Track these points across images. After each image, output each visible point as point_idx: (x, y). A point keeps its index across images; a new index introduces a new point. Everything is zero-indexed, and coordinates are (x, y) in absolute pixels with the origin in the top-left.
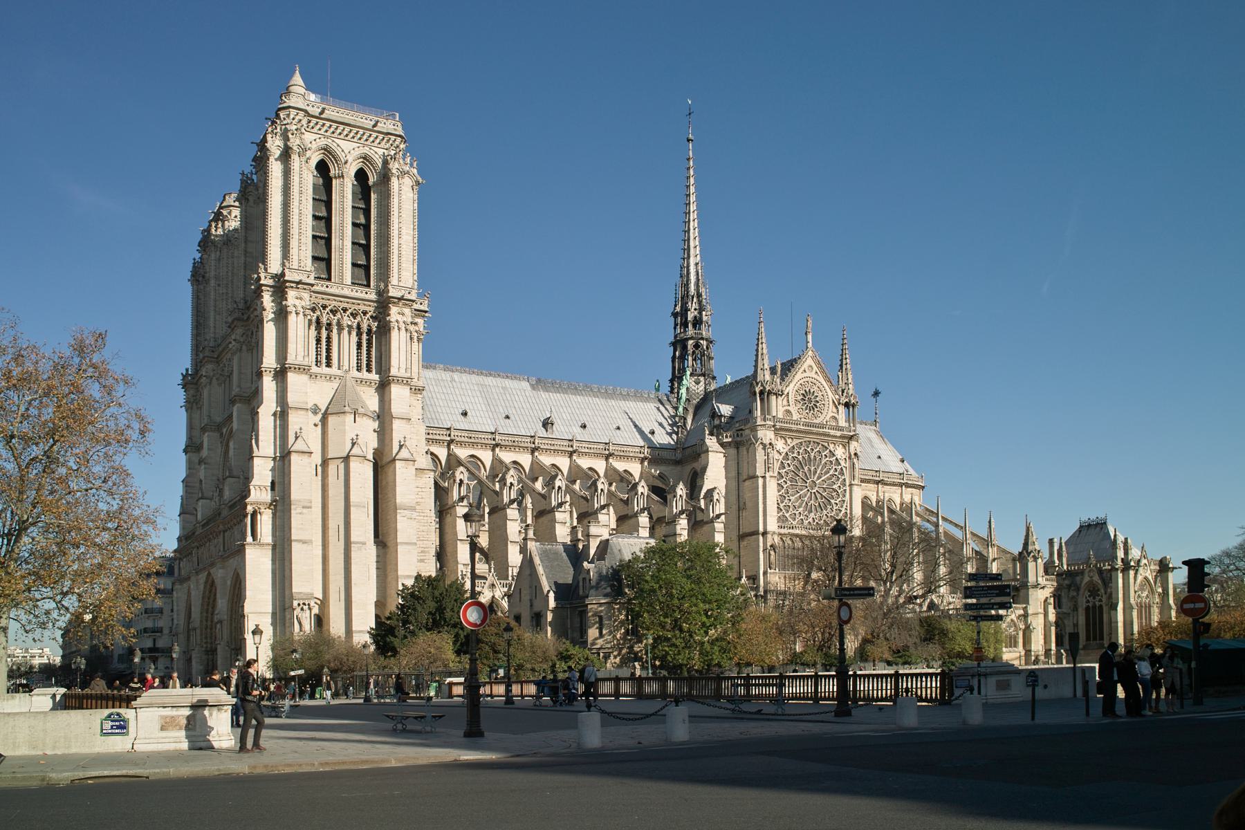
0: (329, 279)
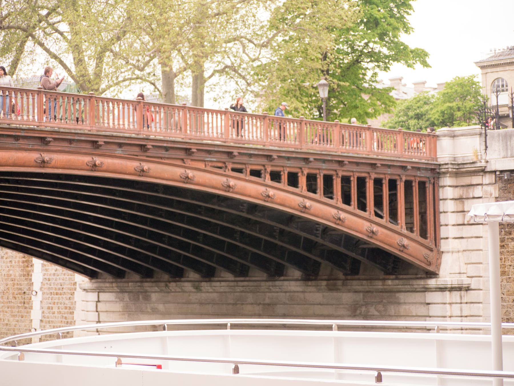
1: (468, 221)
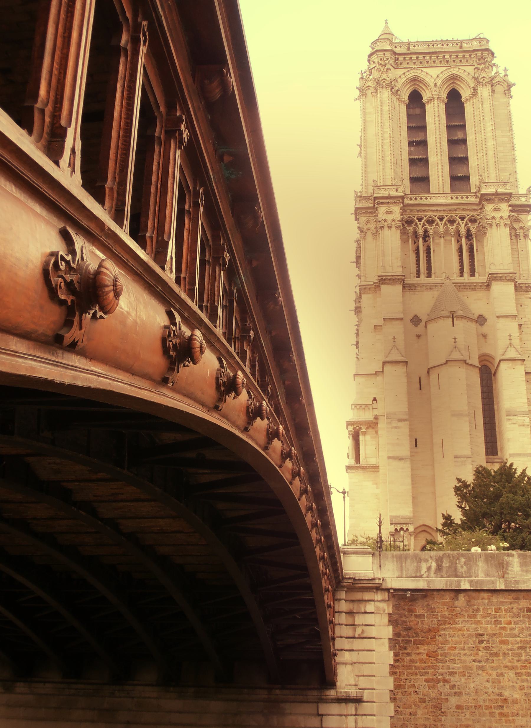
1: (359, 635)
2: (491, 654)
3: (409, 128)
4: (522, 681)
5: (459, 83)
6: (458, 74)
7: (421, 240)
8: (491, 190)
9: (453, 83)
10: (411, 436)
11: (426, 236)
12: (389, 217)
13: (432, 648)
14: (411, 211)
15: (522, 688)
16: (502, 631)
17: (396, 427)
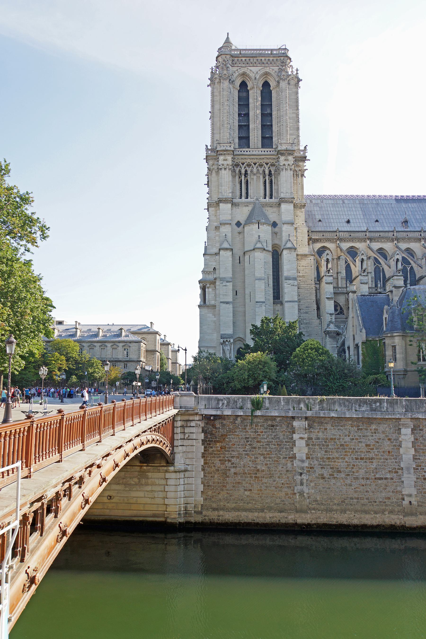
0: (249, 147)
2: (252, 448)
3: (239, 105)
4: (267, 461)
5: (269, 77)
6: (269, 71)
7: (243, 176)
8: (284, 147)
9: (266, 77)
10: (233, 290)
11: (246, 174)
12: (225, 163)
13: (224, 444)
14: (238, 159)
15: (266, 465)
16: (258, 436)
17: (225, 286)
